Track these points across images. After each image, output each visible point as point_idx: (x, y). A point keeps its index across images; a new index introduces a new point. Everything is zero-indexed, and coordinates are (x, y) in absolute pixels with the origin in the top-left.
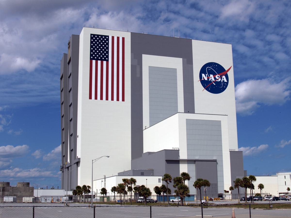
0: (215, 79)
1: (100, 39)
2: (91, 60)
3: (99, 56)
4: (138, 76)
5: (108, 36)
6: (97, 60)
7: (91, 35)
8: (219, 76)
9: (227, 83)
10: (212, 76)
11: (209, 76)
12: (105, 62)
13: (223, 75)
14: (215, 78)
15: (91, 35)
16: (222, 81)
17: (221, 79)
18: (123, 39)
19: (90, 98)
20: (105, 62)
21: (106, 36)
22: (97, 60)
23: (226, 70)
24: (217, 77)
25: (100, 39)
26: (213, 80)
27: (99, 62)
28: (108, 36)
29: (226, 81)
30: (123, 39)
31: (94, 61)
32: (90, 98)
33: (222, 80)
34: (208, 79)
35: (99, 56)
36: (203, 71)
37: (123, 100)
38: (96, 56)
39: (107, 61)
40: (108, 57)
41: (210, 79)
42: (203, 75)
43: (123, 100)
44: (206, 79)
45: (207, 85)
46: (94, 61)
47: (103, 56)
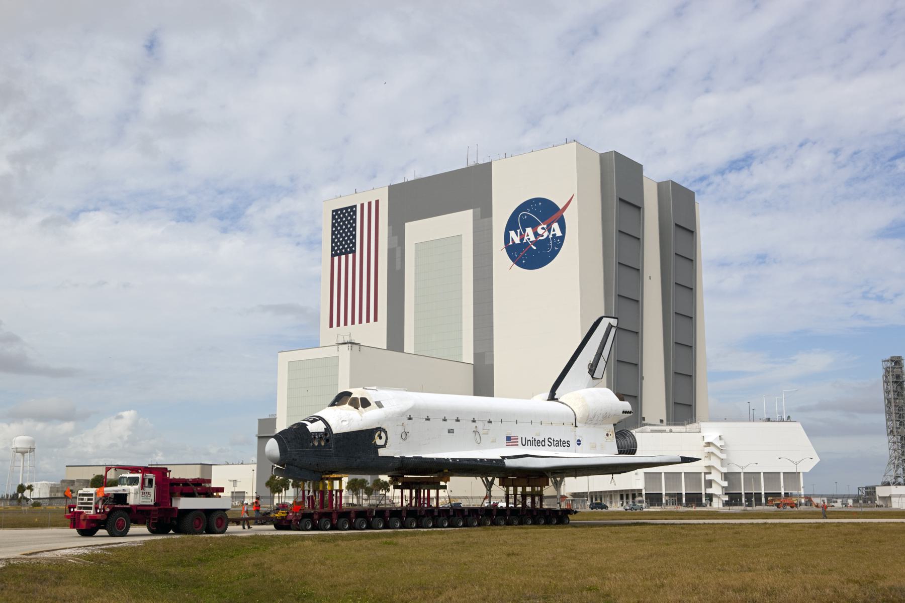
0: (536, 237)
1: (344, 214)
2: (333, 256)
3: (344, 247)
4: (398, 267)
5: (355, 206)
6: (339, 255)
7: (333, 211)
8: (545, 226)
9: (562, 238)
10: (529, 230)
11: (525, 231)
12: (350, 256)
13: (553, 222)
14: (536, 234)
15: (333, 211)
16: (551, 236)
17: (549, 232)
18: (377, 202)
19: (331, 326)
20: (350, 256)
21: (351, 207)
22: (341, 254)
23: (561, 208)
24: (540, 231)
25: (344, 214)
26: (533, 238)
27: (343, 257)
28: (355, 206)
29: (559, 234)
30: (377, 202)
31: (336, 258)
32: (331, 326)
33: (552, 233)
34: (522, 240)
35: (343, 246)
36: (512, 225)
37: (376, 320)
38: (339, 249)
39: (354, 252)
40: (354, 245)
41: (526, 238)
42: (512, 233)
43: (376, 320)
44: (517, 240)
45: (519, 254)
46: (336, 258)
47: (349, 246)
